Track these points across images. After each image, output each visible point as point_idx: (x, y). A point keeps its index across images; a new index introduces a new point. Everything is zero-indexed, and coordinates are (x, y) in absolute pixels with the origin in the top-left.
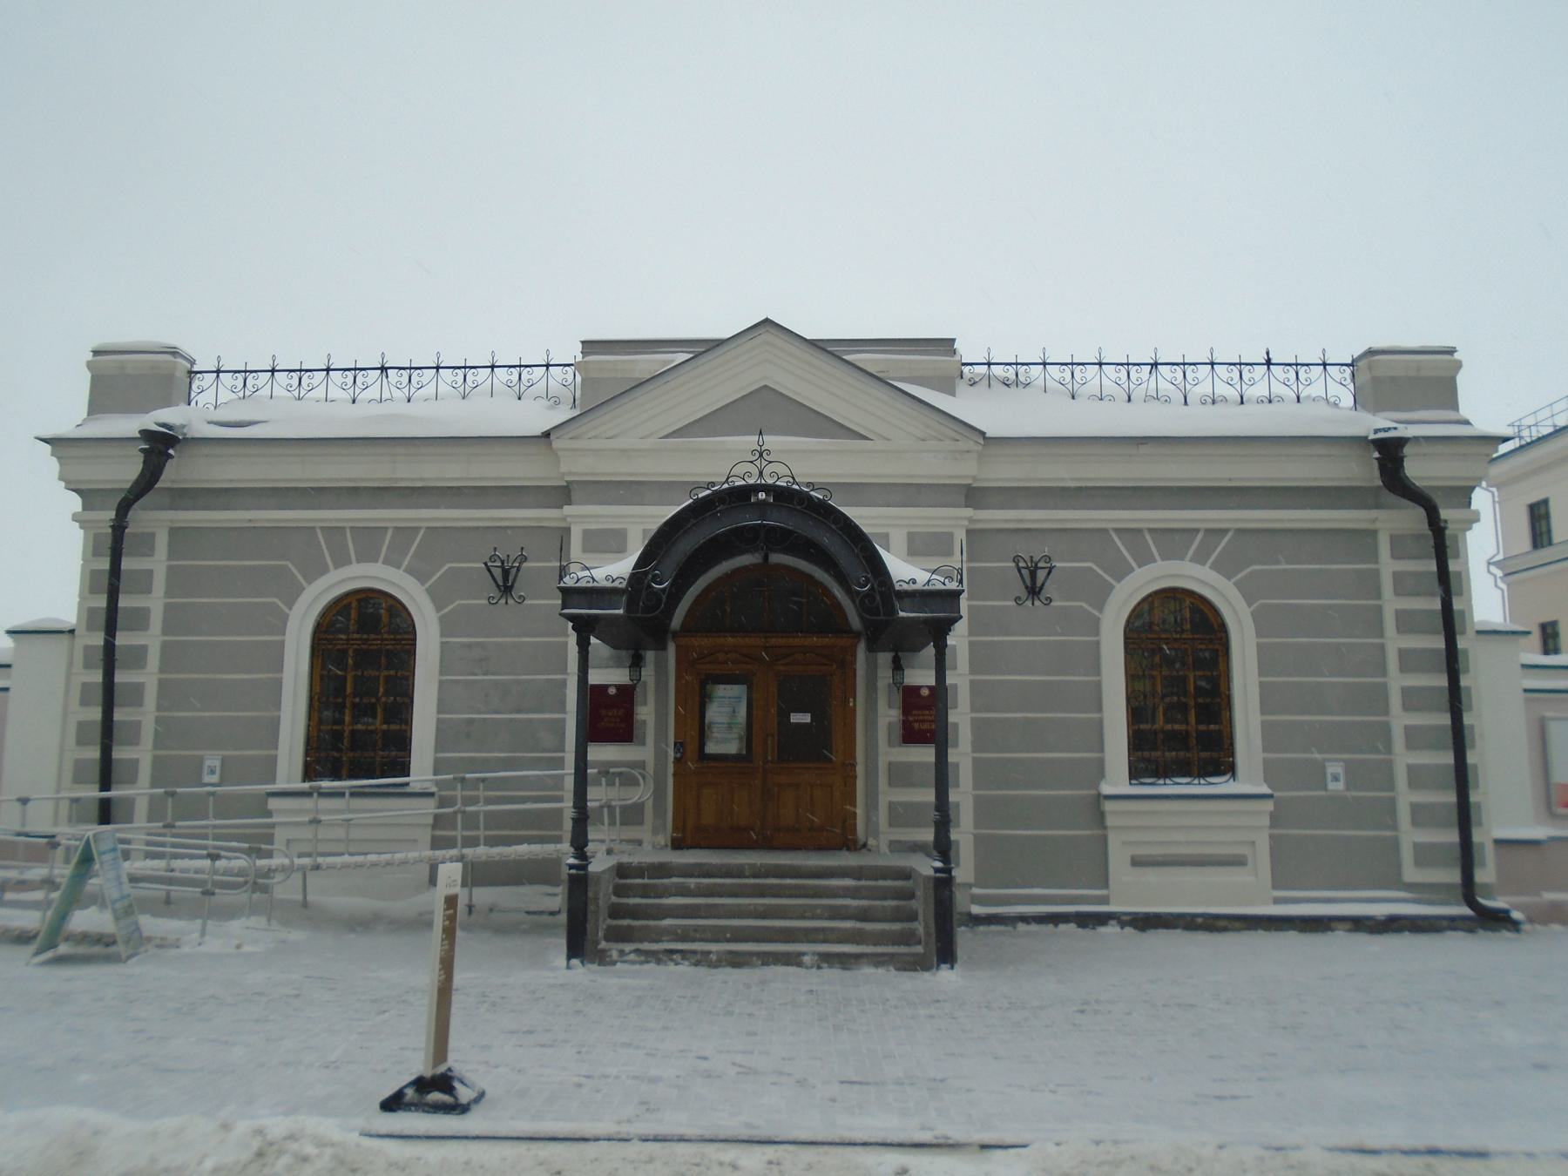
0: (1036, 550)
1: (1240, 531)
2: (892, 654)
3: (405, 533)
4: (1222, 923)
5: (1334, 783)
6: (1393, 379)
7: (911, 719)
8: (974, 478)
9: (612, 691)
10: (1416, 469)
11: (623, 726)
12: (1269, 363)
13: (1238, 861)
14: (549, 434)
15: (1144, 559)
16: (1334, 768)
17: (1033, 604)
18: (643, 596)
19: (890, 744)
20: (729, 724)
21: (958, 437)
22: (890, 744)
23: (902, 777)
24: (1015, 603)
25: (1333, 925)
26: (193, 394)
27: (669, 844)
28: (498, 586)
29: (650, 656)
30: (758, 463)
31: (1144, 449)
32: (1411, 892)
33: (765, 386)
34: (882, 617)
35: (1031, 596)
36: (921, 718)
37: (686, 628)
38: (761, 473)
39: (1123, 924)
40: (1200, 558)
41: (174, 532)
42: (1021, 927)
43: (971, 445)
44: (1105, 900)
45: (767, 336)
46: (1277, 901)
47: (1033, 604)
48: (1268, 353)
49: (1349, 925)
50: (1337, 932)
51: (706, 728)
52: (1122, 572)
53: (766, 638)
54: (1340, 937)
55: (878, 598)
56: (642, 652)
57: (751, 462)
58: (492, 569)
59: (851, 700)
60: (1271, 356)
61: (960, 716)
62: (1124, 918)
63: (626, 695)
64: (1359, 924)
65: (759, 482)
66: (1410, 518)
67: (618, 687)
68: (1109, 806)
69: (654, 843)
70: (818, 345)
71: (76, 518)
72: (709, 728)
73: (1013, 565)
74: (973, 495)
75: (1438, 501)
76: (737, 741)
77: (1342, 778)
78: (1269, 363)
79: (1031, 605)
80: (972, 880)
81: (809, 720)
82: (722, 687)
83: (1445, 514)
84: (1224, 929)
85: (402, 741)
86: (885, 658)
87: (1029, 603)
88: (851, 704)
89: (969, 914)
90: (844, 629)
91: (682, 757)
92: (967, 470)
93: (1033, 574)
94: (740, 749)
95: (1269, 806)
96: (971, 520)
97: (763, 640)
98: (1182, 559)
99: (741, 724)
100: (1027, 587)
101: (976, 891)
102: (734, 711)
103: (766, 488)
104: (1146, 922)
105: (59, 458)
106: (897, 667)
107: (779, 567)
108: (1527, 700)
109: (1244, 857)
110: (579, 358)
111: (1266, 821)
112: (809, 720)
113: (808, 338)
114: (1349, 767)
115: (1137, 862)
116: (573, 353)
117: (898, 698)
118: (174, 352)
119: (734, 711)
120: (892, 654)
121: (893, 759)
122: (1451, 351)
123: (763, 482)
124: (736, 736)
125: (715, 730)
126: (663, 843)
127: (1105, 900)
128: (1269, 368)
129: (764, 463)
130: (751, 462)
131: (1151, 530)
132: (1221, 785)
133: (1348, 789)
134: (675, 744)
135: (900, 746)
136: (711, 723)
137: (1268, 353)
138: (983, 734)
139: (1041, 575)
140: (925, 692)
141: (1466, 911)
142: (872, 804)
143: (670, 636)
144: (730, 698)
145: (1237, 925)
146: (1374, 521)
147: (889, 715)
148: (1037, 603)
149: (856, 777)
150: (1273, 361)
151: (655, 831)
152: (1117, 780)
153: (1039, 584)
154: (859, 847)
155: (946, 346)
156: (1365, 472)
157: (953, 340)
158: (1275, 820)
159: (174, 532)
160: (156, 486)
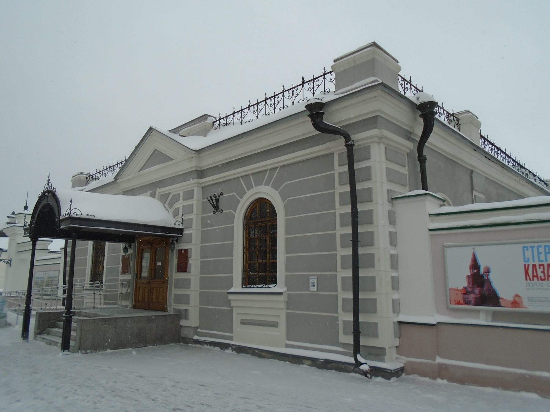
4: (264, 354)
5: (313, 287)
6: (344, 71)
12: (303, 83)
13: (275, 325)
16: (313, 280)
19: (176, 273)
22: (176, 273)
24: (213, 214)
25: (304, 361)
31: (242, 140)
32: (346, 349)
39: (233, 350)
42: (206, 346)
44: (231, 338)
46: (287, 346)
48: (303, 79)
49: (309, 362)
50: (305, 366)
54: (305, 367)
56: (131, 244)
59: (168, 256)
61: (194, 262)
62: (233, 347)
64: (314, 362)
68: (230, 297)
73: (207, 200)
74: (201, 174)
77: (311, 284)
80: (197, 325)
81: (161, 264)
83: (354, 137)
84: (264, 357)
88: (168, 258)
89: (192, 339)
94: (147, 275)
98: (262, 185)
101: (199, 330)
104: (240, 350)
108: (431, 236)
109: (277, 323)
111: (283, 306)
114: (319, 278)
115: (243, 322)
118: (81, 174)
124: (147, 270)
127: (231, 338)
132: (273, 289)
133: (318, 290)
136: (143, 266)
137: (303, 79)
138: (204, 267)
141: (352, 360)
145: (269, 355)
146: (329, 148)
152: (237, 286)
155: (205, 117)
158: (289, 305)
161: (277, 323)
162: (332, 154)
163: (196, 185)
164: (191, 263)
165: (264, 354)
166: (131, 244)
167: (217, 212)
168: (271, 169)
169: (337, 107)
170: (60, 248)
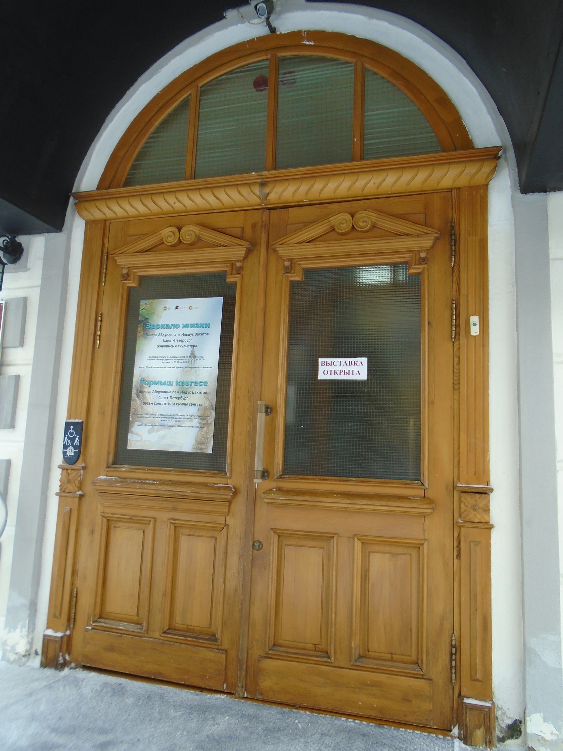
20: (181, 384)
27: (39, 646)
51: (134, 395)
56: (21, 239)
59: (475, 319)
69: (5, 643)
72: (141, 392)
76: (196, 423)
81: (363, 376)
82: (171, 303)
88: (475, 331)
91: (78, 456)
94: (200, 443)
97: (256, 190)
99: (206, 384)
102: (193, 356)
112: (363, 376)
119: (193, 356)
124: (193, 411)
125: (150, 398)
126: (22, 648)
134: (68, 425)
136: (144, 382)
143: (72, 200)
144: (185, 326)
149: (488, 527)
154: (497, 733)
166: (21, 239)
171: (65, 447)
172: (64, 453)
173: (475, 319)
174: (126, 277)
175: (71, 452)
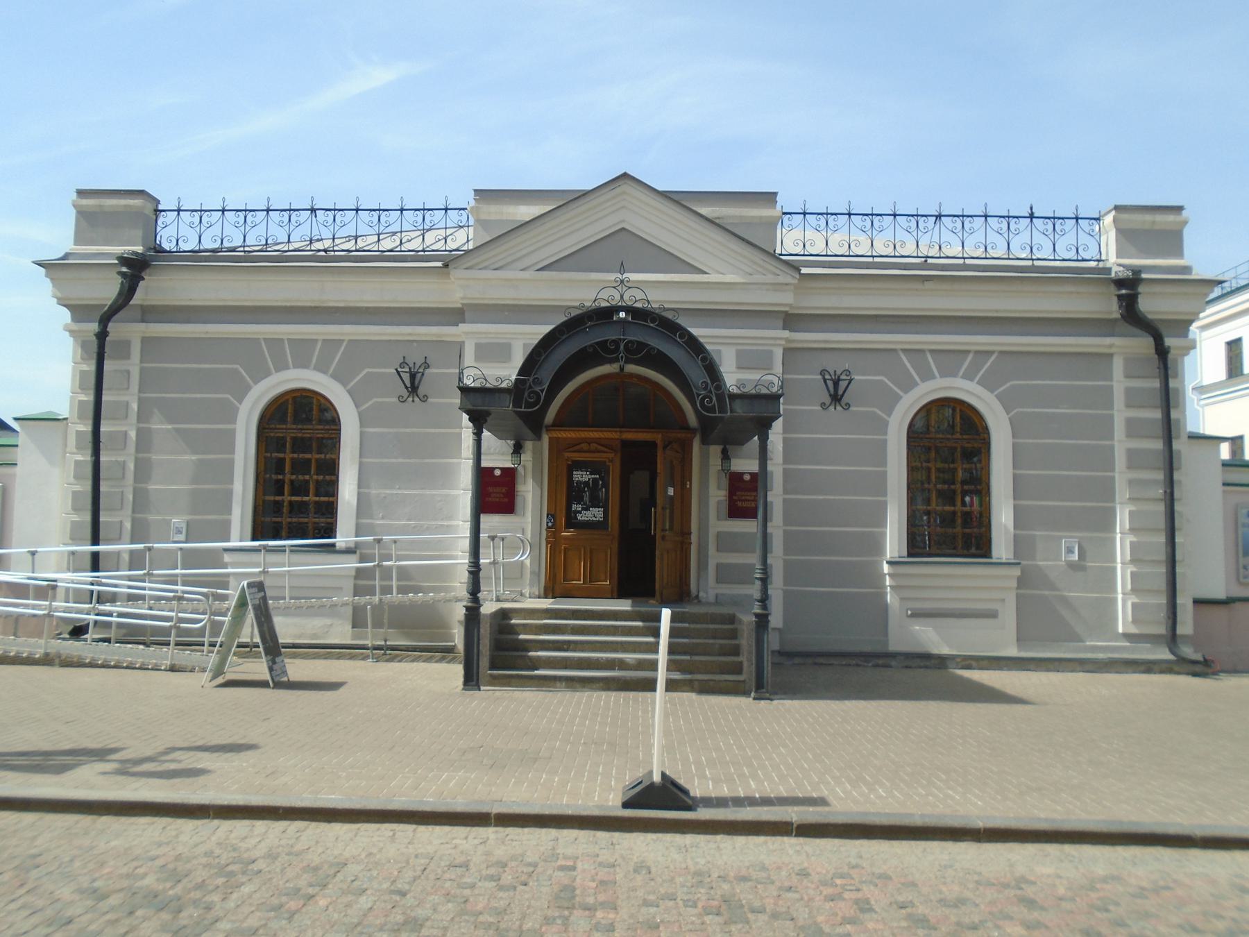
0: (835, 365)
1: (1001, 352)
2: (721, 447)
3: (331, 344)
7: (735, 498)
8: (790, 306)
9: (497, 473)
10: (1148, 305)
11: (506, 500)
12: (1032, 216)
13: (992, 615)
14: (448, 265)
15: (927, 376)
17: (835, 409)
18: (526, 394)
19: (719, 519)
21: (778, 272)
22: (719, 519)
23: (727, 543)
26: (159, 229)
28: (406, 387)
29: (529, 445)
30: (619, 288)
33: (623, 229)
34: (717, 415)
35: (834, 402)
36: (743, 498)
37: (558, 423)
38: (622, 297)
40: (969, 376)
41: (145, 341)
43: (789, 280)
45: (626, 187)
47: (835, 409)
48: (1031, 208)
52: (909, 385)
53: (621, 432)
55: (714, 398)
57: (614, 287)
58: (402, 374)
59: (688, 483)
60: (1033, 211)
61: (776, 496)
63: (509, 475)
65: (620, 304)
66: (1143, 344)
67: (502, 469)
70: (666, 195)
71: (67, 328)
73: (820, 377)
74: (791, 320)
75: (1164, 331)
78: (1032, 216)
79: (833, 410)
83: (1169, 341)
85: (330, 509)
86: (715, 450)
87: (832, 408)
88: (688, 486)
90: (685, 426)
92: (785, 300)
93: (836, 383)
95: (1016, 572)
96: (787, 340)
97: (618, 433)
100: (830, 395)
103: (628, 309)
105: (52, 279)
106: (726, 456)
107: (631, 375)
108: (1224, 492)
110: (473, 203)
111: (1015, 584)
113: (660, 189)
116: (467, 200)
117: (725, 482)
120: (721, 447)
121: (720, 529)
122: (1179, 209)
123: (624, 304)
128: (1031, 221)
129: (625, 289)
130: (614, 287)
131: (932, 351)
135: (726, 520)
137: (1031, 208)
139: (843, 385)
140: (747, 477)
142: (703, 565)
143: (544, 430)
146: (1111, 346)
147: (717, 495)
148: (839, 408)
150: (1035, 215)
151: (531, 585)
153: (840, 392)
155: (769, 198)
156: (1108, 306)
157: (775, 194)
159: (145, 341)
160: (131, 303)
161: (997, 611)
162: (1111, 356)
163: (783, 342)
164: (772, 503)
165: (985, 663)
167: (832, 408)
168: (977, 352)
169: (1157, 288)
170: (15, 416)
171: (547, 523)
172: (547, 525)
173: (688, 483)
174: (567, 460)
175: (550, 524)
